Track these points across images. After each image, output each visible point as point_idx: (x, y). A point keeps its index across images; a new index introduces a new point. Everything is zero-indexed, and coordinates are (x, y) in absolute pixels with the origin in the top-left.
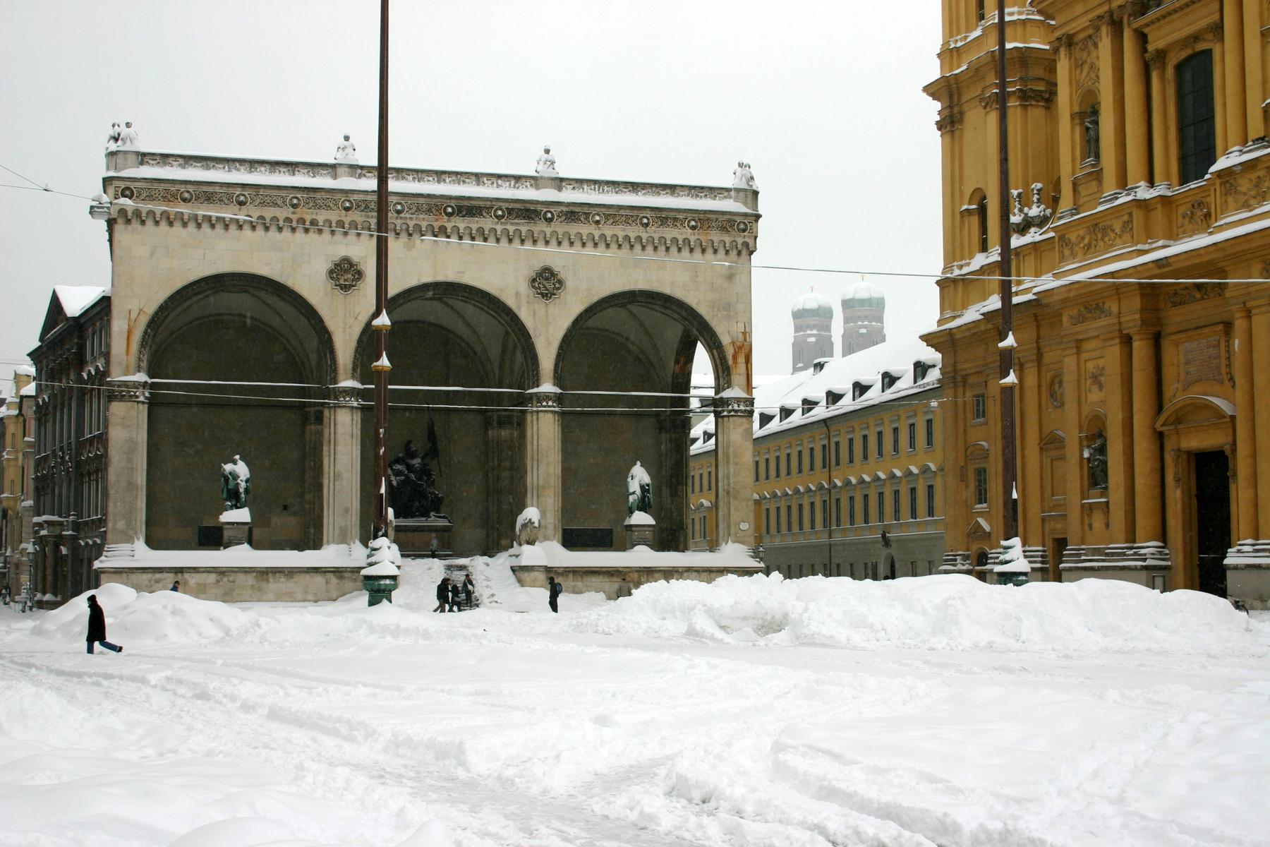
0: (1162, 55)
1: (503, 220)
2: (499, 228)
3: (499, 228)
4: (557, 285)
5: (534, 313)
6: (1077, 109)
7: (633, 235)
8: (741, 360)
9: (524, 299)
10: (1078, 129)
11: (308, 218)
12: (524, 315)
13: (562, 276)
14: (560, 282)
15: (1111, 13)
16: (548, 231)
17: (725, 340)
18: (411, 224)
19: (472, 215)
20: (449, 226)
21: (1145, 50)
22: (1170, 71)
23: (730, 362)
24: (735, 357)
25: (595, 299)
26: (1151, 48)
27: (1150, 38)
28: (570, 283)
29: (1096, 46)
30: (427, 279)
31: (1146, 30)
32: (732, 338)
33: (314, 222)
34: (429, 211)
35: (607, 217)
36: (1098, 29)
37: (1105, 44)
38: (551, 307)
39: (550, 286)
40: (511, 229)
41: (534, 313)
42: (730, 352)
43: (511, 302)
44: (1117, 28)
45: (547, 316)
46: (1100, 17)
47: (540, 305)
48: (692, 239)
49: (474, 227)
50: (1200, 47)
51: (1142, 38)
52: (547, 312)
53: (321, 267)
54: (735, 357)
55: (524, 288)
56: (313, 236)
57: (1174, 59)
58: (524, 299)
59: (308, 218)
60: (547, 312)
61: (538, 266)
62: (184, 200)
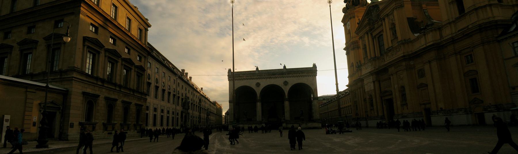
0: (375, 36)
2: (278, 76)
6: (363, 47)
7: (298, 75)
10: (364, 51)
11: (253, 78)
12: (283, 88)
14: (288, 83)
15: (366, 32)
16: (285, 76)
17: (313, 89)
18: (266, 77)
19: (274, 75)
20: (271, 77)
21: (372, 36)
22: (377, 39)
23: (314, 92)
24: (315, 91)
25: (293, 84)
26: (373, 36)
27: (373, 34)
29: (365, 37)
30: (269, 84)
31: (372, 33)
33: (253, 78)
34: (268, 75)
35: (294, 73)
36: (365, 35)
37: (366, 36)
40: (280, 76)
42: (314, 91)
43: (281, 86)
44: (367, 33)
46: (365, 33)
48: (307, 75)
49: (275, 76)
50: (381, 34)
51: (372, 34)
53: (255, 84)
55: (283, 84)
56: (253, 80)
57: (377, 37)
59: (253, 78)
61: (285, 81)
62: (237, 77)
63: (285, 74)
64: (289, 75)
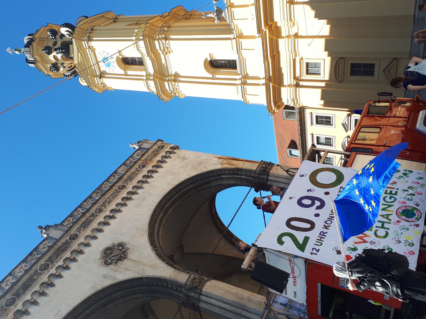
1: (50, 266)
3: (53, 271)
4: (120, 248)
5: (126, 269)
8: (235, 162)
9: (112, 273)
13: (117, 242)
25: (146, 227)
28: (123, 239)
32: (219, 164)
38: (130, 256)
39: (116, 252)
41: (126, 269)
43: (107, 283)
45: (134, 261)
47: (125, 263)
52: (131, 260)
54: (231, 165)
58: (112, 273)
60: (131, 260)
63: (74, 237)
64: (94, 225)
